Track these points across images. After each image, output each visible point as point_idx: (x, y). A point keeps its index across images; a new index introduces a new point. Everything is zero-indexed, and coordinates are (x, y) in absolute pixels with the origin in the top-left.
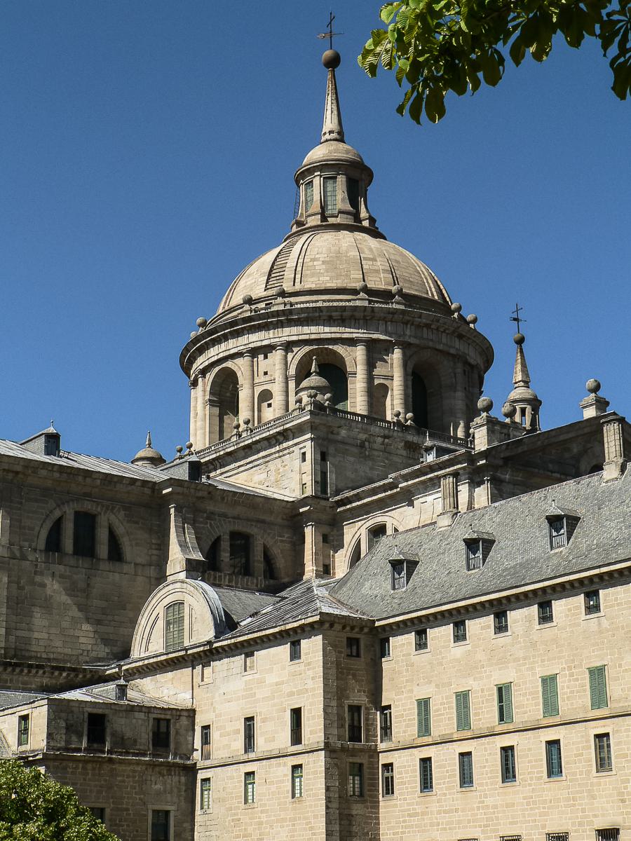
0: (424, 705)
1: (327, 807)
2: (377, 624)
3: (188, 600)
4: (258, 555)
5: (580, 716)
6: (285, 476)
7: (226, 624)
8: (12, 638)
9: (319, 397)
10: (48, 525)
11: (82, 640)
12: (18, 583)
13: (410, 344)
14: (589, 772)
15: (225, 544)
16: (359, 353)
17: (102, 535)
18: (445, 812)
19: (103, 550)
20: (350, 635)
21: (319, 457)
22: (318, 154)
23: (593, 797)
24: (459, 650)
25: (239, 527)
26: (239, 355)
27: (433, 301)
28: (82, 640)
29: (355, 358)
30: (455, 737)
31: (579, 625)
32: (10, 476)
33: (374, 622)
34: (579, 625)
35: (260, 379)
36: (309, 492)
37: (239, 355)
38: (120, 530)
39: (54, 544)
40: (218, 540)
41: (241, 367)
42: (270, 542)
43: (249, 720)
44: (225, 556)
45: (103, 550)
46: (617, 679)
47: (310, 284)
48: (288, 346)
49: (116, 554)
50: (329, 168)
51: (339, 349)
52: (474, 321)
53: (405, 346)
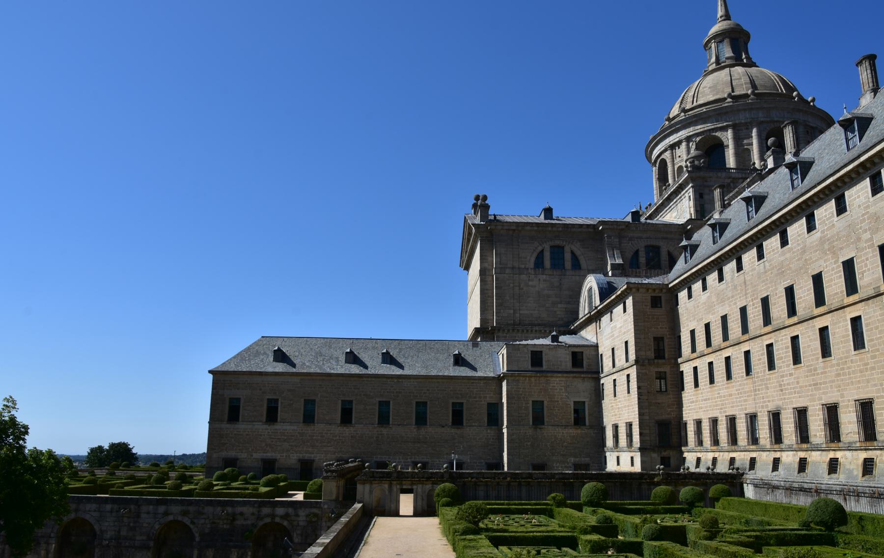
0: (693, 332)
1: (639, 399)
2: (670, 286)
4: (664, 257)
5: (758, 333)
8: (518, 315)
9: (696, 163)
10: (535, 255)
11: (558, 313)
12: (519, 286)
13: (762, 122)
14: (764, 371)
16: (730, 133)
17: (568, 256)
18: (705, 400)
19: (568, 264)
20: (654, 295)
21: (698, 196)
22: (715, 29)
23: (767, 388)
24: (704, 296)
26: (665, 150)
27: (781, 95)
28: (558, 313)
29: (728, 137)
30: (706, 352)
31: (755, 269)
32: (511, 232)
33: (668, 285)
34: (755, 269)
35: (677, 160)
37: (665, 150)
38: (578, 253)
39: (539, 263)
40: (637, 252)
41: (667, 156)
42: (671, 249)
43: (613, 349)
44: (642, 260)
45: (568, 264)
46: (775, 304)
47: (701, 102)
48: (688, 139)
50: (720, 37)
51: (718, 134)
52: (813, 100)
53: (760, 125)
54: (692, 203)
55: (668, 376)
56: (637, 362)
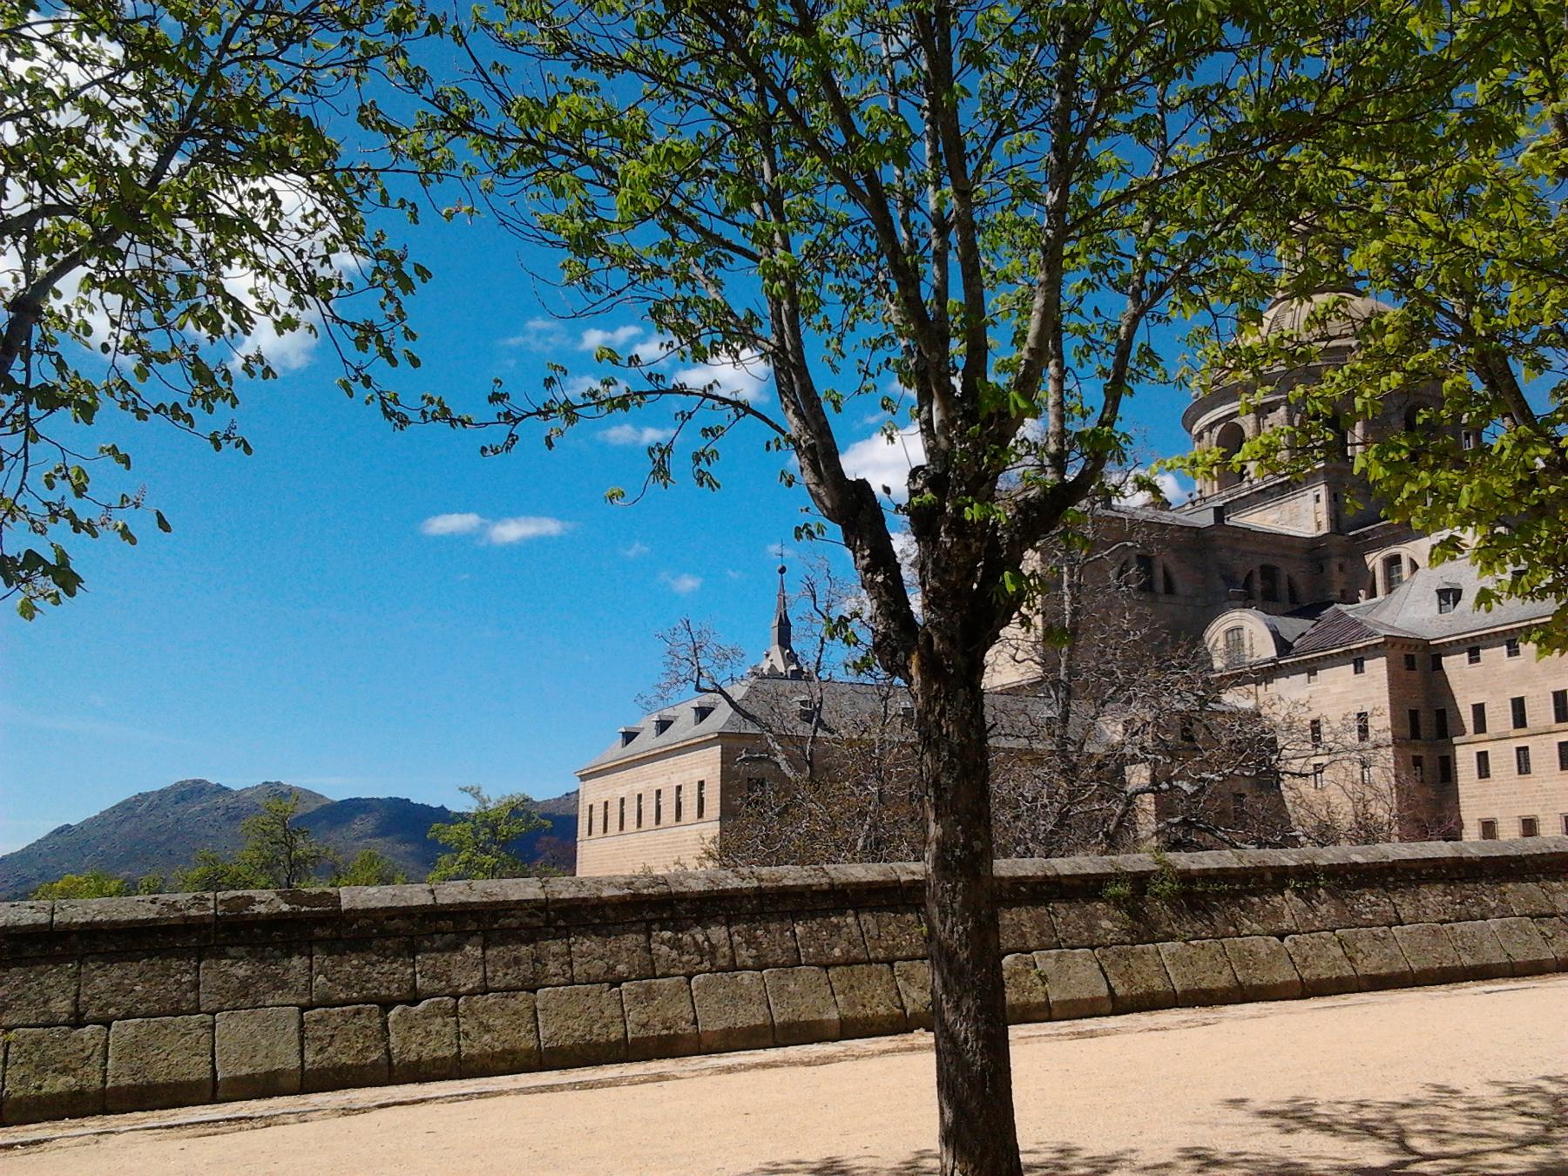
3: (1248, 627)
4: (1283, 586)
6: (1303, 516)
7: (1283, 646)
15: (1257, 577)
19: (1160, 586)
25: (1270, 561)
36: (1325, 530)
38: (1173, 568)
44: (1258, 586)
45: (1160, 586)
49: (1170, 589)
54: (1323, 505)
55: (1426, 763)
56: (1398, 742)
